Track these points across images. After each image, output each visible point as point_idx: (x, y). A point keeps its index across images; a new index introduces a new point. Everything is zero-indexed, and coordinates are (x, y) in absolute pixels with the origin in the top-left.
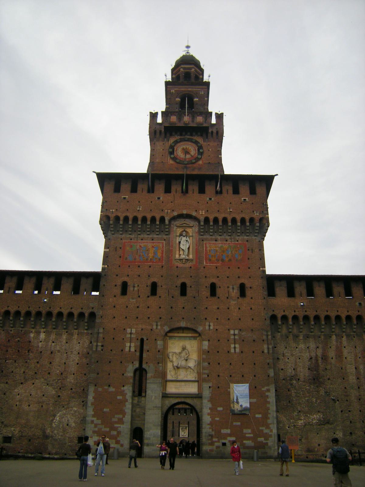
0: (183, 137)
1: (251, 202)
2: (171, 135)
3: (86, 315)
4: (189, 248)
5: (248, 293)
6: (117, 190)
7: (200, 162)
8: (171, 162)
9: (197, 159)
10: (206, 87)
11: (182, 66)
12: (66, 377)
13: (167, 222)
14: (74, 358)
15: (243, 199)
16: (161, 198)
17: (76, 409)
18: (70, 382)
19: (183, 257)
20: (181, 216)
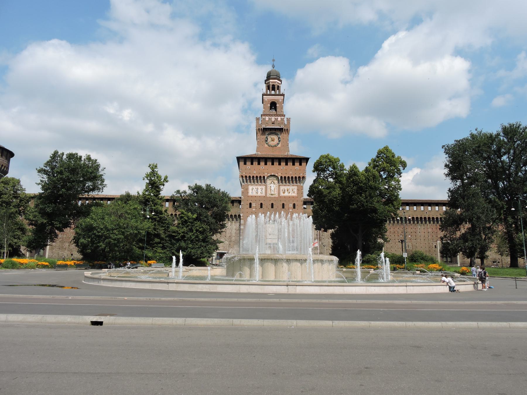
0: (272, 132)
1: (299, 170)
2: (266, 130)
3: (237, 216)
4: (274, 189)
5: (296, 207)
6: (245, 164)
7: (279, 146)
8: (266, 146)
9: (278, 144)
10: (283, 97)
11: (271, 81)
12: (232, 238)
13: (266, 179)
14: (234, 231)
15: (296, 168)
16: (263, 168)
17: (236, 248)
18: (233, 239)
19: (272, 193)
20: (271, 176)
